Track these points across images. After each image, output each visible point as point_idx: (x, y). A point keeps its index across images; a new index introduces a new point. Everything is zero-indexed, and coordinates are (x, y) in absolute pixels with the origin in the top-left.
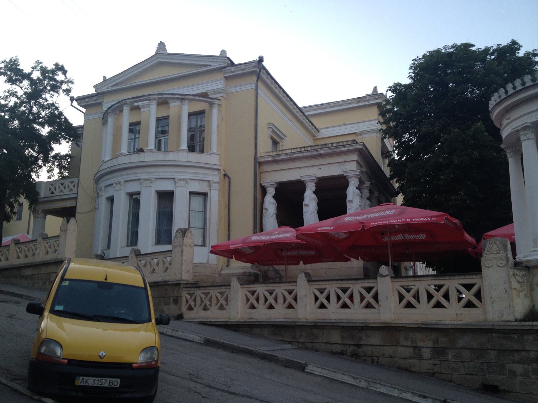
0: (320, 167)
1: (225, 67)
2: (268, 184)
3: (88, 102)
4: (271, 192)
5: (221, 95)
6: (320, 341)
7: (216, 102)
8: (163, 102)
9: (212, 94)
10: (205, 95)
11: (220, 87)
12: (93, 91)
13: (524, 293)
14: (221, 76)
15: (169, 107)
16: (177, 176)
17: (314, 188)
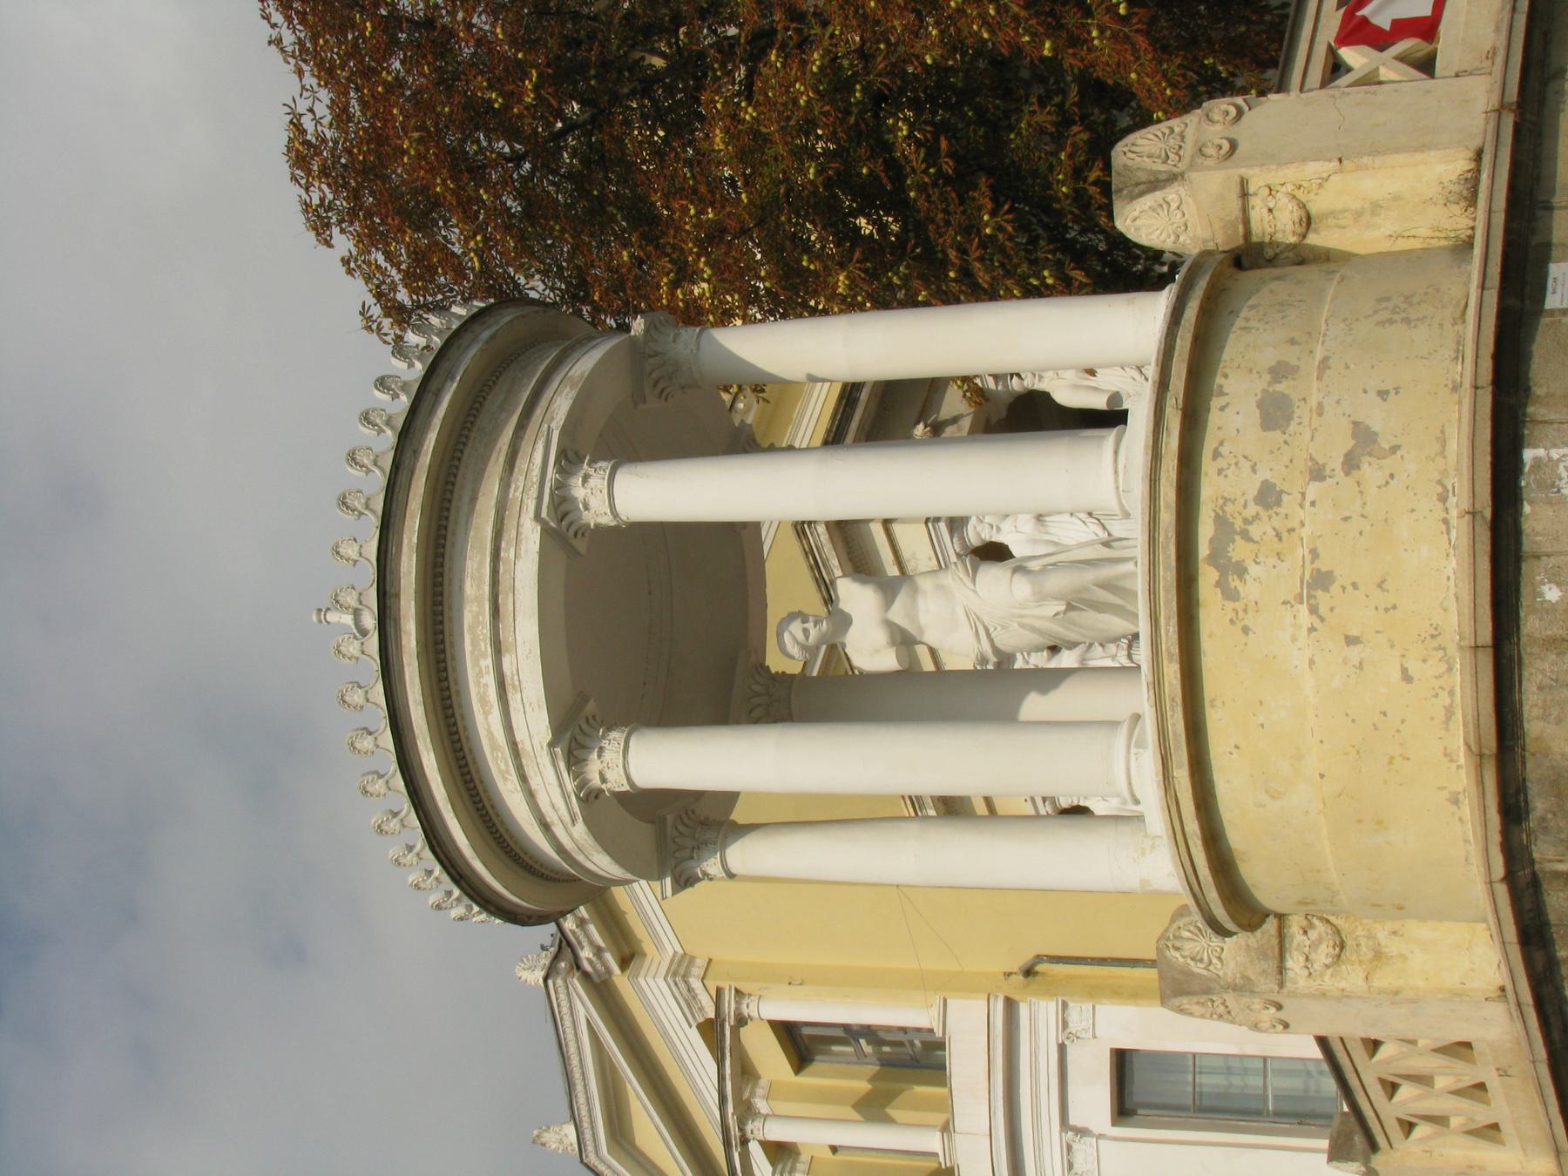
1: (586, 976)
5: (696, 984)
9: (701, 1009)
10: (711, 1031)
13: (1382, 935)
14: (620, 980)
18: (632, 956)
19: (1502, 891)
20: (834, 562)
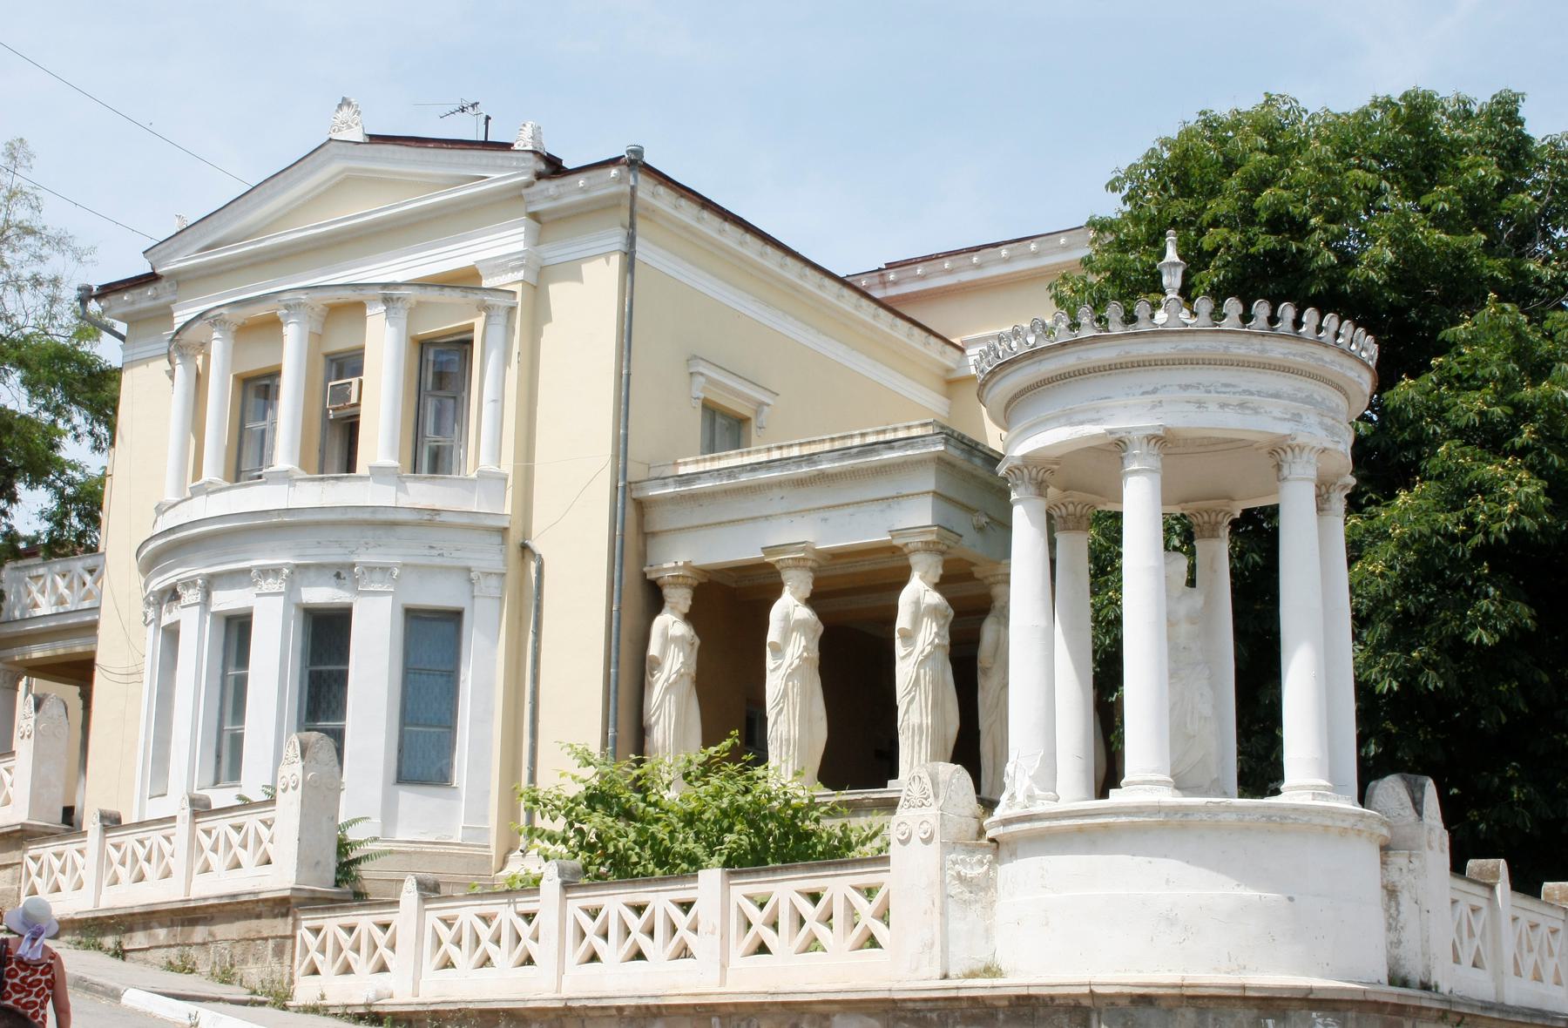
0: (826, 514)
1: (529, 185)
3: (133, 303)
4: (678, 599)
7: (501, 301)
8: (346, 309)
9: (492, 275)
10: (465, 281)
11: (520, 247)
12: (146, 269)
15: (364, 318)
16: (363, 558)
17: (806, 589)
18: (539, 221)
19: (1086, 990)
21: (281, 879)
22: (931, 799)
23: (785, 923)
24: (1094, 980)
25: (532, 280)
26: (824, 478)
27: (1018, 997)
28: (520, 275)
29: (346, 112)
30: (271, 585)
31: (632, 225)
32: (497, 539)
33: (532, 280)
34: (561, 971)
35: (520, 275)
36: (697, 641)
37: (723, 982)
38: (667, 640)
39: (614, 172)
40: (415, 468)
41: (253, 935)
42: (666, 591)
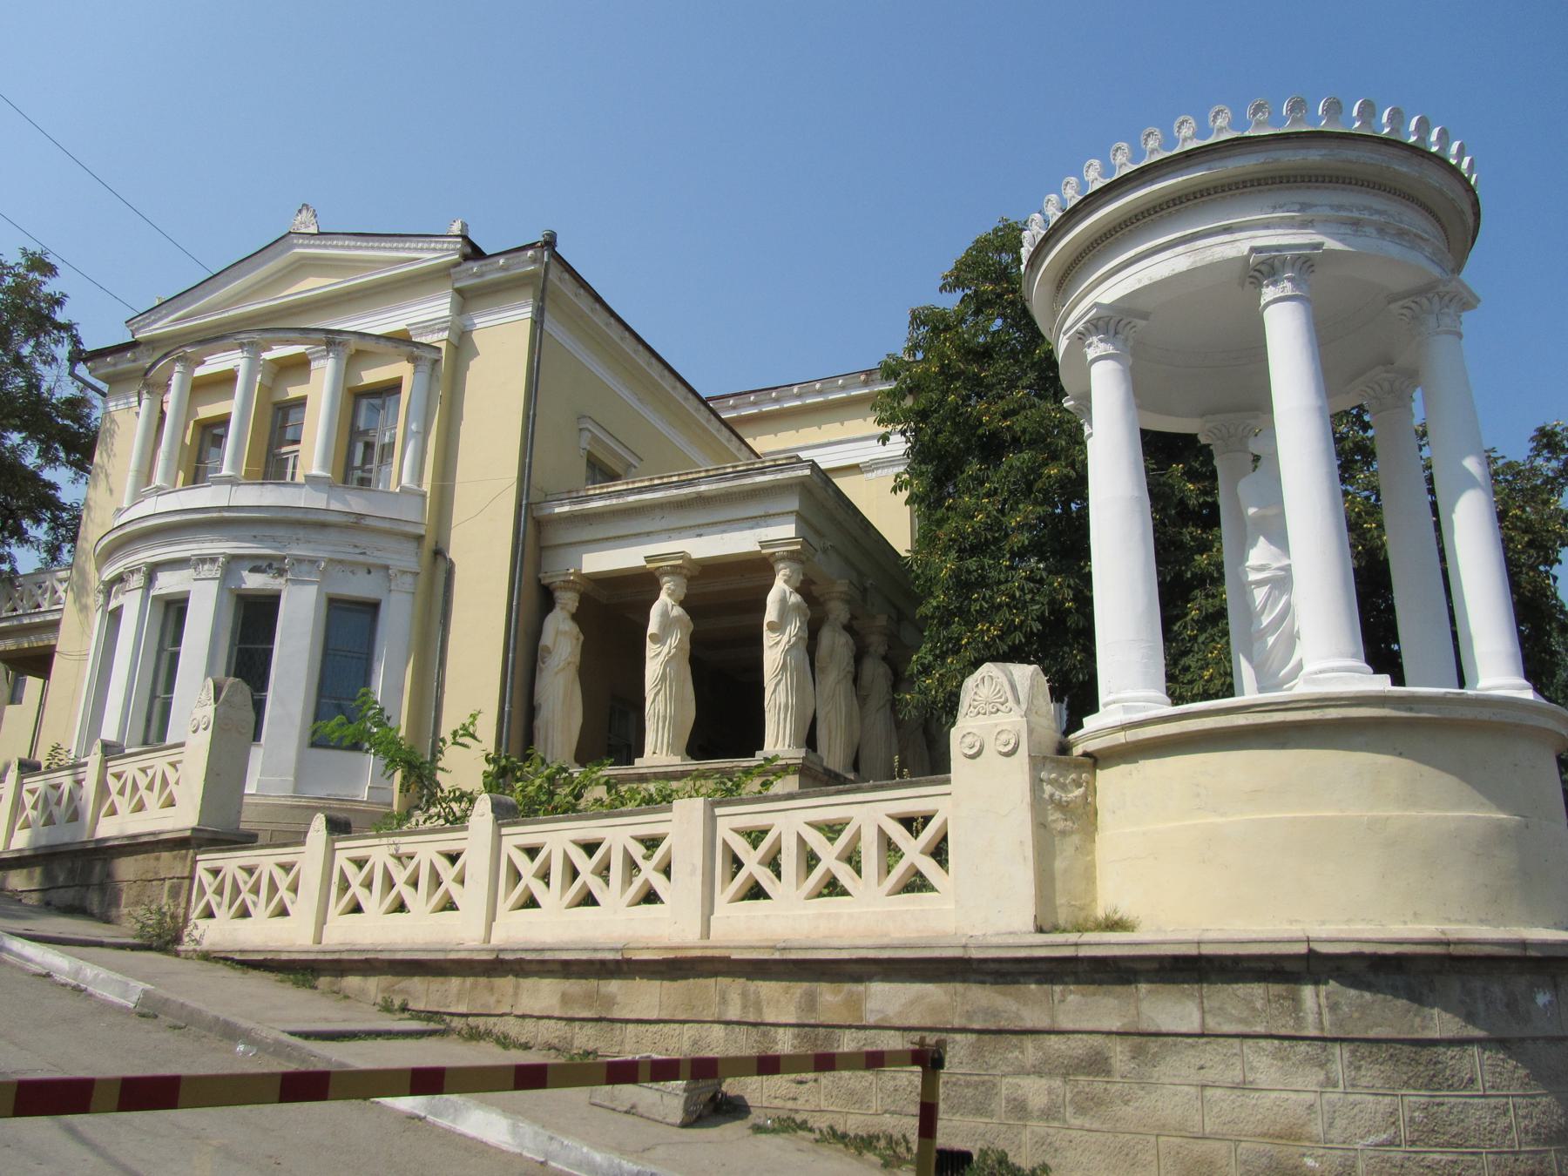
1: (456, 265)
2: (558, 580)
4: (568, 601)
6: (507, 1009)
9: (421, 335)
10: (401, 342)
11: (447, 313)
17: (681, 593)
19: (1302, 949)
20: (779, 476)
21: (184, 817)
22: (1011, 703)
23: (789, 861)
24: (1312, 935)
25: (455, 342)
26: (702, 501)
27: (1176, 959)
28: (445, 335)
29: (305, 215)
30: (206, 570)
31: (542, 299)
32: (412, 546)
33: (455, 342)
34: (492, 916)
35: (445, 335)
36: (582, 638)
37: (706, 933)
38: (558, 632)
39: (530, 253)
40: (345, 481)
41: (150, 876)
42: (558, 594)
